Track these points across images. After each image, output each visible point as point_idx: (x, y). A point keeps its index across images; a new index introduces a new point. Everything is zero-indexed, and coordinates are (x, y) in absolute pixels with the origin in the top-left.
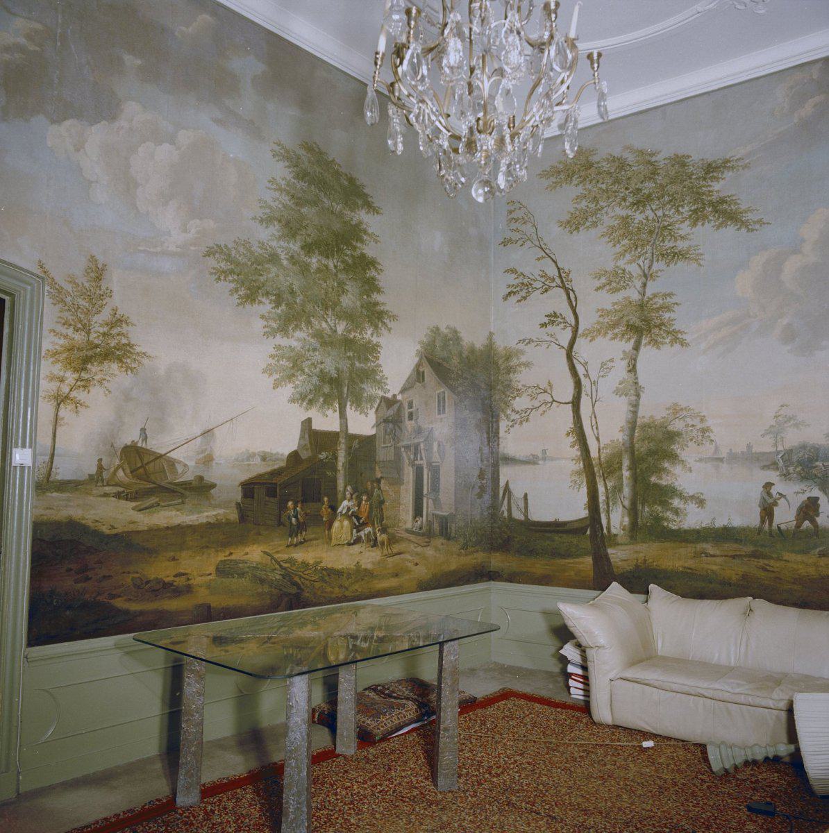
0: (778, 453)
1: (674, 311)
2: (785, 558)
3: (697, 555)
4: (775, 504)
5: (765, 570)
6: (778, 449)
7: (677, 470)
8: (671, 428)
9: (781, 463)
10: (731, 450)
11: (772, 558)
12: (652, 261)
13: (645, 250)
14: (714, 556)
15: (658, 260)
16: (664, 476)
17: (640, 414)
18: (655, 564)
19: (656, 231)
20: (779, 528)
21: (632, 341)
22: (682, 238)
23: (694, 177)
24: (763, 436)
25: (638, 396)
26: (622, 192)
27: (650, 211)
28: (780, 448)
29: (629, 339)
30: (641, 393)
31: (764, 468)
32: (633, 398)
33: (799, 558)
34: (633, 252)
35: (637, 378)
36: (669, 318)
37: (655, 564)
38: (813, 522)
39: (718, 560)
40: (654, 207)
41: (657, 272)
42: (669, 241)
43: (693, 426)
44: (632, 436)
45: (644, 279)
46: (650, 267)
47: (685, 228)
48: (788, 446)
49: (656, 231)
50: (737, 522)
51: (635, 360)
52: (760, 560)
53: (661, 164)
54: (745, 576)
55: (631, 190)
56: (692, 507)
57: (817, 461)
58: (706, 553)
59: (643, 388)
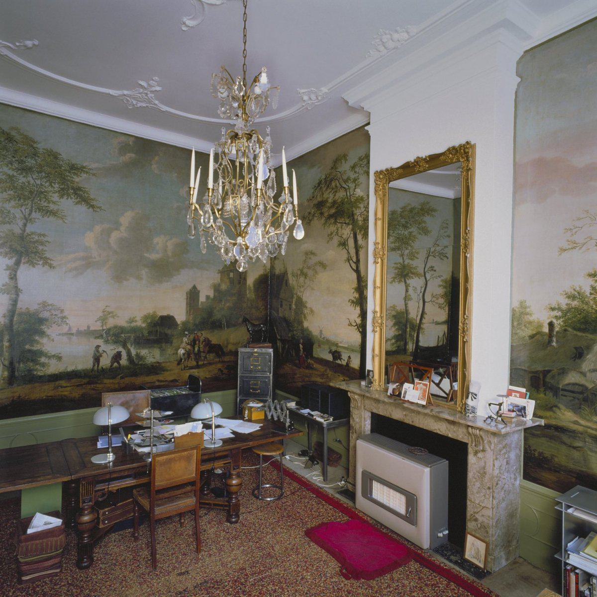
0: (103, 330)
1: (45, 246)
2: (104, 382)
3: (56, 388)
4: (101, 356)
5: (93, 389)
6: (104, 328)
7: (45, 340)
8: (41, 316)
9: (105, 335)
10: (78, 329)
11: (97, 383)
12: (31, 211)
13: (27, 203)
14: (66, 387)
15: (36, 212)
16: (35, 345)
17: (19, 305)
18: (27, 397)
19: (35, 193)
20: (102, 368)
21: (14, 259)
22: (54, 203)
23: (63, 168)
24: (96, 321)
25: (18, 295)
26: (9, 158)
27: (31, 178)
28: (105, 328)
29: (12, 258)
30: (20, 293)
31: (96, 338)
32: (14, 296)
33: (111, 381)
34: (17, 202)
35: (17, 283)
36: (42, 249)
37: (27, 397)
38: (118, 363)
39: (68, 389)
40: (34, 177)
41: (35, 219)
42: (44, 202)
43: (55, 315)
44: (11, 321)
45: (25, 221)
46: (30, 214)
47: (55, 197)
48: (108, 327)
49: (35, 193)
50: (80, 367)
51: (16, 272)
52: (92, 385)
53: (41, 151)
54: (83, 395)
55: (16, 159)
56: (53, 362)
57: (122, 334)
58: (61, 386)
59: (22, 290)
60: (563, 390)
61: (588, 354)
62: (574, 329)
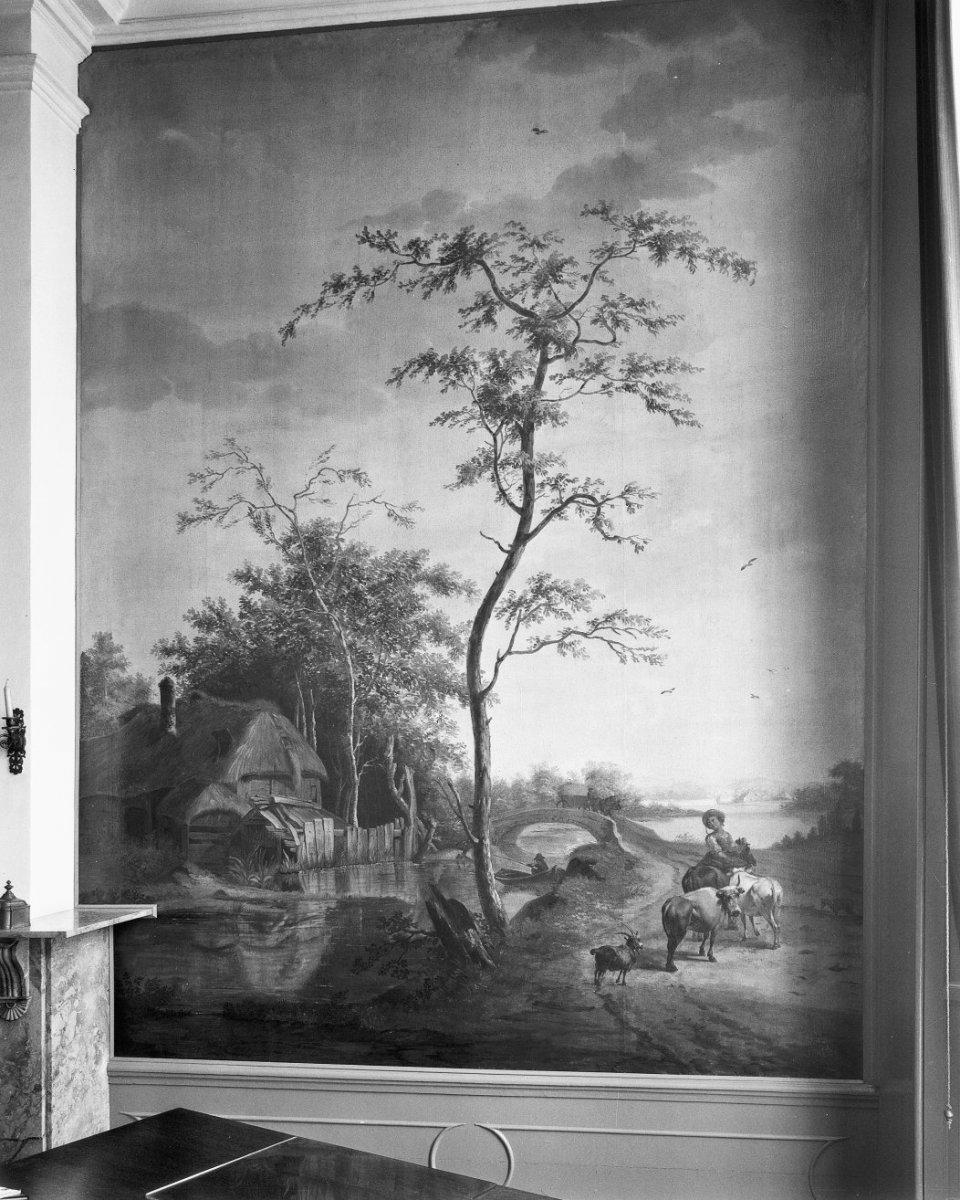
60: (193, 829)
61: (238, 745)
62: (211, 692)
